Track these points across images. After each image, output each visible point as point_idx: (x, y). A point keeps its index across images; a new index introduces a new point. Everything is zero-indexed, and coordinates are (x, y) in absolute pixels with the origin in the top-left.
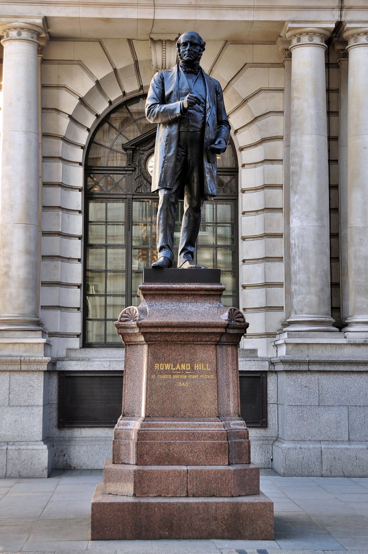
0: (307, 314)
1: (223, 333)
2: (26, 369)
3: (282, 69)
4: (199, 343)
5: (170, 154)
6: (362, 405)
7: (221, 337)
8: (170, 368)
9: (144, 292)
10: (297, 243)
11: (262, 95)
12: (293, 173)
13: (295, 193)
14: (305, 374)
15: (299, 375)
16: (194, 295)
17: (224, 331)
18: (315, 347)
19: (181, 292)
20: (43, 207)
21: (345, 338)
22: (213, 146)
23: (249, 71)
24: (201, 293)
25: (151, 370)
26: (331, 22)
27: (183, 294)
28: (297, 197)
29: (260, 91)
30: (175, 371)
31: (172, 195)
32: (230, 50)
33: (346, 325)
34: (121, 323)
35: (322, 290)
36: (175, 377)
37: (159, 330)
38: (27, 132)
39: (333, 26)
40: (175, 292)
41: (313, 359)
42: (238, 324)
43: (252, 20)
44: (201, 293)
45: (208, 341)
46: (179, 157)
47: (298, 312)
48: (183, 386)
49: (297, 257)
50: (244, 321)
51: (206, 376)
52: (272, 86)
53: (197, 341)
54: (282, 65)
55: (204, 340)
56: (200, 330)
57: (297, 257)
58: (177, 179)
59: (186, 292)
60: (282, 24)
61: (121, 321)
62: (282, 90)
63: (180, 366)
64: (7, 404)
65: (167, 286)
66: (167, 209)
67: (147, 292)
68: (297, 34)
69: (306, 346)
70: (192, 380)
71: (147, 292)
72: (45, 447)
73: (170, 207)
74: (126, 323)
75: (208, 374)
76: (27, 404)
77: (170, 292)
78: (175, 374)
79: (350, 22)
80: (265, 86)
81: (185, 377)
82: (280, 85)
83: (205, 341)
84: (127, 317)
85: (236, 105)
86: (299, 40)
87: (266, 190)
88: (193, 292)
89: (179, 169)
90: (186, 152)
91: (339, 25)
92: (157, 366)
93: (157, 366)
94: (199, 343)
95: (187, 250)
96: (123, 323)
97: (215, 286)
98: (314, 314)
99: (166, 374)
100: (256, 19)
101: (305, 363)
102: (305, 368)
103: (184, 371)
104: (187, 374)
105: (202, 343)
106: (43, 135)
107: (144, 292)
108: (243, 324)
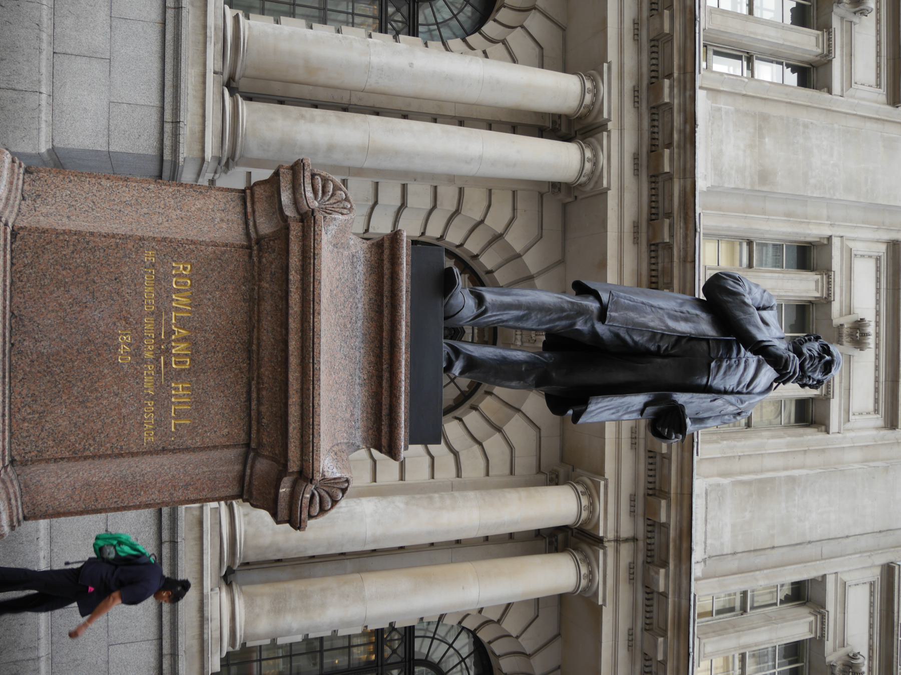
0: (245, 532)
1: (285, 466)
2: (165, 129)
3: (534, 471)
4: (254, 395)
6: (110, 623)
7: (273, 459)
8: (177, 310)
9: (387, 244)
10: (342, 510)
11: (507, 450)
12: (431, 498)
13: (407, 504)
14: (156, 536)
15: (154, 528)
16: (380, 378)
17: (293, 467)
18: (196, 549)
19: (386, 343)
20: (377, 183)
21: (212, 590)
23: (532, 432)
24: (385, 394)
25: (172, 248)
26: (605, 531)
27: (381, 347)
28: (402, 506)
30: (168, 322)
31: (589, 325)
33: (229, 585)
34: (308, 174)
35: (279, 550)
36: (149, 324)
37: (294, 277)
39: (601, 534)
40: (386, 327)
41: (180, 547)
42: (306, 501)
43: (607, 436)
44: (385, 394)
45: (259, 422)
47: (247, 518)
48: (118, 346)
50: (311, 517)
51: (150, 418)
52: (517, 461)
53: (259, 390)
54: (539, 471)
55: (263, 409)
56: (294, 399)
58: (617, 335)
59: (386, 356)
60: (601, 472)
61: (313, 176)
62: (512, 472)
63: (184, 339)
64: (112, 99)
65: (404, 306)
66: (562, 310)
67: (387, 252)
69: (198, 535)
70: (138, 377)
71: (387, 252)
72: (43, 149)
73: (567, 318)
74: (309, 188)
75: (158, 423)
76: (112, 128)
77: (386, 312)
78: (158, 323)
79: (605, 554)
80: (517, 453)
81: (148, 355)
82: (518, 470)
83: (259, 413)
84: (324, 193)
85: (492, 419)
86: (583, 493)
88: (386, 375)
89: (637, 338)
90: (666, 355)
91: (599, 541)
92: (183, 268)
93: (183, 268)
94: (254, 395)
95: (457, 358)
96: (308, 181)
97: (403, 433)
98: (245, 541)
99: (158, 296)
101: (174, 536)
102: (166, 536)
103: (168, 351)
104: (157, 360)
105: (254, 403)
106: (460, 189)
107: (387, 244)
108: (305, 515)
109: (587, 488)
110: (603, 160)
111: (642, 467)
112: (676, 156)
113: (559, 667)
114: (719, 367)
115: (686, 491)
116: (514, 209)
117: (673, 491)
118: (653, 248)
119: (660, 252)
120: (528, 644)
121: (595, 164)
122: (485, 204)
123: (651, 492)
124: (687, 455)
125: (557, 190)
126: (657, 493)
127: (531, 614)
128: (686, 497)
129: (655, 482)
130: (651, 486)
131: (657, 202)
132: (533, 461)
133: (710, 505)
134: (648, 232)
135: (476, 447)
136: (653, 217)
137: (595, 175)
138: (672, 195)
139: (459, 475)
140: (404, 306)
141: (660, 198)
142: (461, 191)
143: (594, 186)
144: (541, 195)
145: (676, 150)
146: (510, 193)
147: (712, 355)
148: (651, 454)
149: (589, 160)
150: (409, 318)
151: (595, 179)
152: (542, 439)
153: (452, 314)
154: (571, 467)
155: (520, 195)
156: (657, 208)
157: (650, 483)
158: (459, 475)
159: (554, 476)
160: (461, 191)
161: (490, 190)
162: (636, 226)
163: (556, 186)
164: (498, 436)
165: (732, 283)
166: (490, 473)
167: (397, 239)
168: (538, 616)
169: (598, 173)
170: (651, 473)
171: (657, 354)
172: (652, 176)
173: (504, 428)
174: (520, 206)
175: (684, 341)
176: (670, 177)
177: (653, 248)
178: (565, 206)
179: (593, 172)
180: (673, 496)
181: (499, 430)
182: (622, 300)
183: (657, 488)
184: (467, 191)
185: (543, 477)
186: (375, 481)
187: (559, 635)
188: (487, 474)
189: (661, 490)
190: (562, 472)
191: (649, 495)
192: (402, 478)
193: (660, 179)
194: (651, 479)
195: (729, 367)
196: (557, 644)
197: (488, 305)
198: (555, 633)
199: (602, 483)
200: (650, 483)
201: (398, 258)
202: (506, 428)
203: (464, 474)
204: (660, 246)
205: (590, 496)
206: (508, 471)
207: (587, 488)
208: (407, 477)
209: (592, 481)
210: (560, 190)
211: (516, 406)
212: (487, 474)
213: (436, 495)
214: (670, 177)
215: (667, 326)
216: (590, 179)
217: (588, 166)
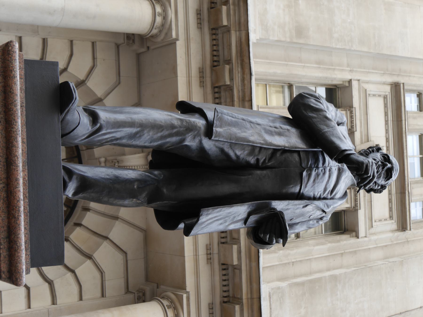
3: (123, 291)
23: (120, 257)
29: (102, 273)
31: (197, 140)
32: (138, 235)
38: (63, 10)
46: (257, 150)
52: (107, 284)
54: (128, 291)
58: (222, 151)
60: (182, 287)
65: (19, 121)
66: (173, 127)
73: (177, 134)
80: (107, 276)
82: (108, 292)
85: (83, 248)
86: (169, 307)
89: (238, 153)
95: (70, 178)
97: (23, 256)
100: (187, 259)
109: (172, 302)
110: (171, 15)
111: (217, 278)
112: (232, 12)
114: (309, 176)
115: (255, 296)
116: (94, 58)
117: (244, 297)
118: (216, 90)
119: (223, 94)
121: (165, 18)
122: (68, 53)
123: (226, 300)
124: (254, 264)
125: (131, 42)
126: (231, 300)
128: (256, 301)
129: (228, 291)
130: (225, 294)
131: (217, 51)
132: (122, 282)
133: (273, 306)
134: (211, 77)
135: (69, 275)
136: (215, 64)
137: (165, 28)
138: (230, 45)
139: (54, 302)
140: (19, 121)
141: (220, 48)
142: (44, 42)
143: (164, 38)
144: (118, 46)
145: (231, 7)
146: (90, 44)
147: (303, 165)
148: (224, 267)
149: (159, 14)
150: (25, 134)
151: (165, 31)
152: (129, 262)
153: (67, 132)
154: (155, 285)
155: (98, 46)
156: (218, 56)
157: (225, 291)
158: (54, 302)
159: (141, 294)
160: (44, 42)
161: (72, 42)
162: (201, 71)
163: (130, 38)
164: (89, 263)
165: (314, 101)
167: (9, 51)
169: (167, 26)
170: (225, 283)
171: (256, 166)
172: (213, 29)
173: (94, 255)
174: (99, 55)
175: (278, 154)
176: (228, 30)
177: (216, 90)
178: (138, 56)
179: (163, 25)
180: (245, 301)
181: (89, 257)
182: (226, 116)
183: (231, 295)
184: (50, 41)
185: (131, 296)
188: (81, 299)
189: (234, 297)
190: (148, 289)
191: (224, 302)
193: (219, 31)
194: (225, 289)
195: (318, 175)
197: (102, 122)
199: (185, 296)
200: (225, 291)
201: (11, 71)
202: (96, 255)
203: (59, 301)
204: (222, 88)
205: (175, 308)
206: (99, 294)
207: (172, 302)
209: (176, 295)
210: (134, 41)
211: (104, 234)
212: (81, 299)
214: (228, 30)
215: (265, 140)
216: (160, 31)
217: (159, 19)
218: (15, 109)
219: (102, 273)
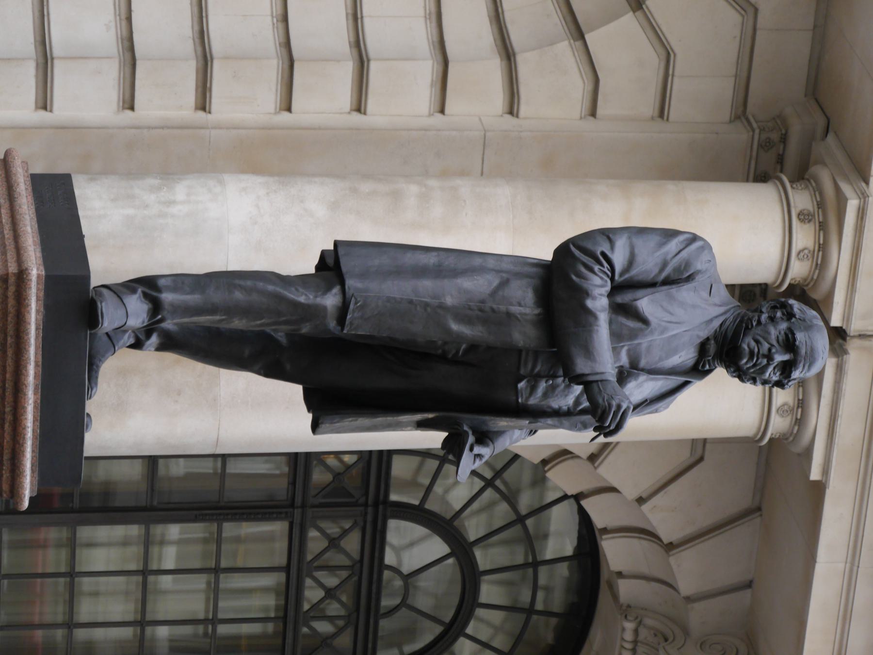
3: (726, 114)
5: (455, 327)
9: (12, 280)
10: (175, 210)
11: (653, 60)
12: (396, 196)
13: (334, 206)
22: (471, 439)
28: (320, 211)
49: (130, 211)
52: (678, 86)
57: (130, 211)
62: (662, 112)
68: (825, 215)
71: (12, 289)
80: (680, 66)
82: (676, 110)
86: (804, 217)
87: (347, 70)
109: (821, 205)
113: (749, 585)
120: (666, 517)
127: (684, 457)
139: (512, 109)
147: (522, 372)
154: (821, 122)
158: (512, 109)
159: (775, 136)
166: (600, 111)
167: (23, 278)
168: (701, 459)
171: (443, 358)
186: (289, 109)
187: (755, 510)
192: (359, 107)
195: (553, 388)
196: (742, 537)
198: (745, 501)
201: (25, 300)
203: (524, 110)
205: (823, 226)
208: (372, 103)
213: (414, 189)
215: (449, 331)
218: (26, 338)
219: (668, 56)
